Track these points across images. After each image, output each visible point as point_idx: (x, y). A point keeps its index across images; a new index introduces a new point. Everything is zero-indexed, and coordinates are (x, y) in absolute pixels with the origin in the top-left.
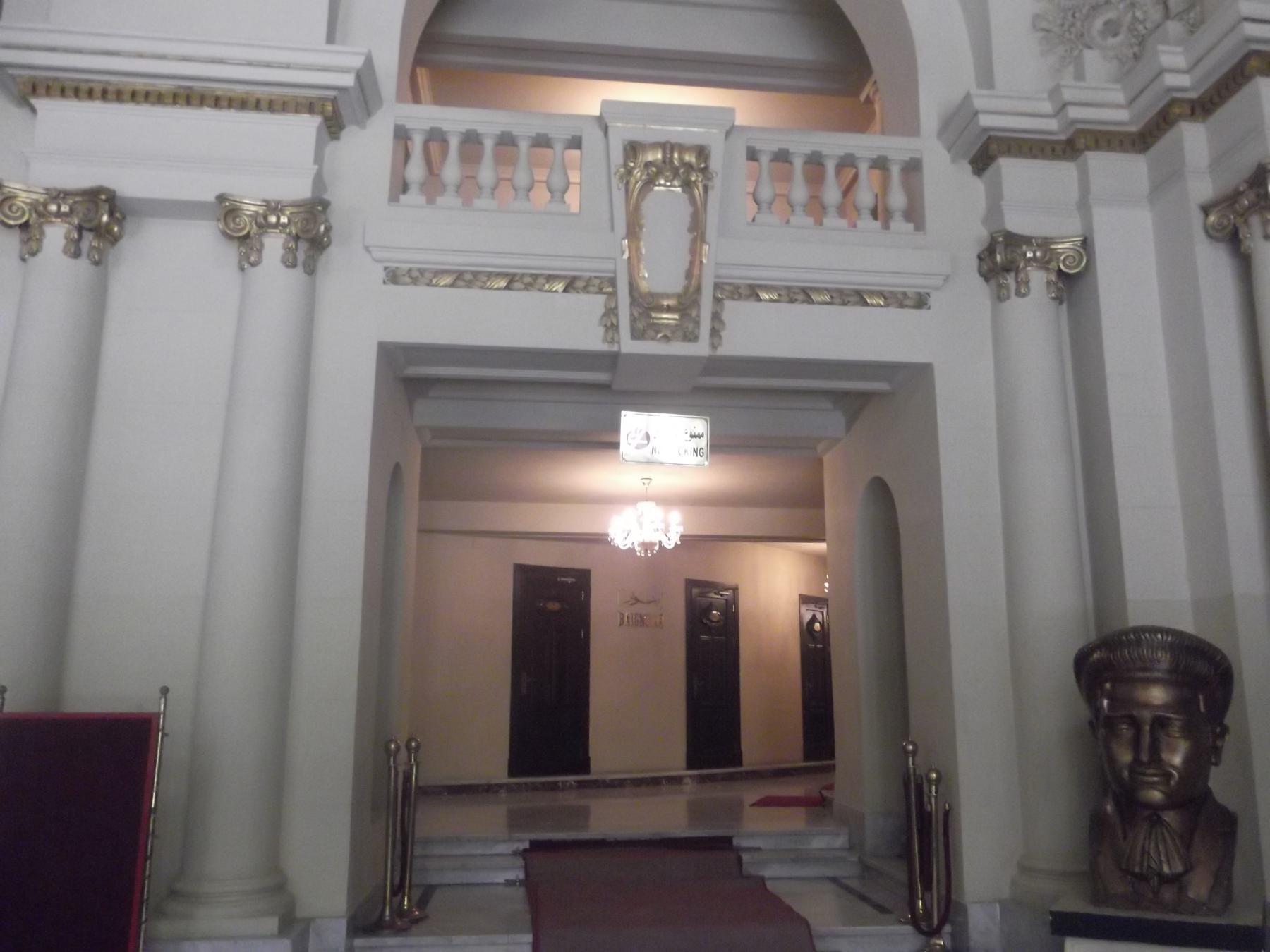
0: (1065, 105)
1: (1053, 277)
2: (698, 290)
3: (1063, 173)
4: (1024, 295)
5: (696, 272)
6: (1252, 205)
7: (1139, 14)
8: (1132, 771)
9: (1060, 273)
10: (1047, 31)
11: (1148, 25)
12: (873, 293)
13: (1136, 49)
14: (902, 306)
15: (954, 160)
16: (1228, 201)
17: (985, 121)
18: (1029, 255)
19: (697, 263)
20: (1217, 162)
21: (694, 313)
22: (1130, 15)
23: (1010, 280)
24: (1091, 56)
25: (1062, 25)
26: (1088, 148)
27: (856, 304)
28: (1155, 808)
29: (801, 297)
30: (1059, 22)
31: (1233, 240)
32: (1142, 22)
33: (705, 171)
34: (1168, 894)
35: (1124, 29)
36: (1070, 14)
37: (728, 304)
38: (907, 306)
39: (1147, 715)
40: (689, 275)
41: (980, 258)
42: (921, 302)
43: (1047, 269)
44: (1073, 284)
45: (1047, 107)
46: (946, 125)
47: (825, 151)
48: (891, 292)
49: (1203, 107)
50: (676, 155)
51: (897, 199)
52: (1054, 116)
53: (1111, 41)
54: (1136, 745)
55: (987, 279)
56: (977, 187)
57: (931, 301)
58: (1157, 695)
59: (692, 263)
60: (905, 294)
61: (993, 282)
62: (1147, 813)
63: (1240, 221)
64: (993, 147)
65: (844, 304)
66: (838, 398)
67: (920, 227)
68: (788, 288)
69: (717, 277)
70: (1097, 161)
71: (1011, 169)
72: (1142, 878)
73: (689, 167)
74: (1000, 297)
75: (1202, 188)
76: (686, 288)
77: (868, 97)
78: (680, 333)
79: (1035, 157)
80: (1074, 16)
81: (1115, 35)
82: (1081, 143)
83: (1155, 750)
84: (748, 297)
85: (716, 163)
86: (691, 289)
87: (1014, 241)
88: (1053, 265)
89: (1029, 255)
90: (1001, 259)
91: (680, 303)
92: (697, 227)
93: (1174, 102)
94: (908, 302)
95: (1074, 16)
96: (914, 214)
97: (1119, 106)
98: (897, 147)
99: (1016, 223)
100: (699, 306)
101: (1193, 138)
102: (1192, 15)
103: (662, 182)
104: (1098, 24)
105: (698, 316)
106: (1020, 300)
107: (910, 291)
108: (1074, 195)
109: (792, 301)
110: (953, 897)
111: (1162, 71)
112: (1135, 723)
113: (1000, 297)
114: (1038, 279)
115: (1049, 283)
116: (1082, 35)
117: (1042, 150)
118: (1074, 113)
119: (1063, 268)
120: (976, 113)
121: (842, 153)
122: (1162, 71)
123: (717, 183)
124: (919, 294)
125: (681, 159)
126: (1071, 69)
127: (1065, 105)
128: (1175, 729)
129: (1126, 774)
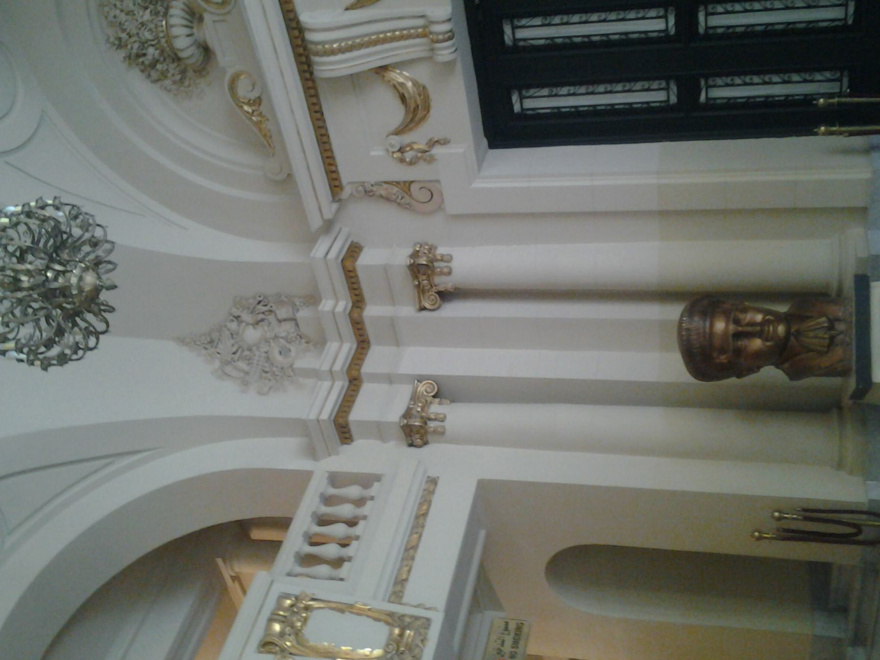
0: (331, 371)
1: (437, 400)
2: (391, 615)
3: (367, 388)
4: (445, 417)
5: (376, 615)
6: (428, 280)
7: (283, 335)
8: (767, 340)
9: (434, 397)
10: (270, 388)
11: (292, 330)
12: (419, 508)
13: (303, 341)
14: (433, 492)
15: (337, 454)
16: (421, 290)
17: (325, 416)
18: (419, 409)
19: (370, 613)
20: (393, 301)
21: (408, 620)
22: (281, 341)
23: (432, 425)
24: (298, 364)
25: (270, 380)
26: (359, 370)
27: (425, 519)
28: (788, 333)
29: (411, 552)
30: (267, 381)
31: (445, 296)
32: (288, 333)
33: (297, 598)
34: (841, 327)
35: (288, 346)
36: (264, 375)
37: (405, 600)
38: (434, 490)
39: (732, 328)
40: (377, 620)
41: (411, 445)
42: (433, 481)
43: (431, 403)
44: (443, 391)
45: (327, 384)
46: (312, 453)
47: (305, 528)
48: (422, 497)
49: (358, 301)
50: (281, 613)
51: (354, 491)
52: (333, 381)
53: (293, 354)
54: (750, 335)
55: (426, 443)
56: (360, 444)
57: (432, 473)
58: (720, 326)
59: (368, 616)
60: (425, 490)
61: (430, 438)
62: (792, 339)
63: (434, 289)
64: (341, 421)
65: (423, 527)
66: (476, 605)
67: (378, 478)
68: (403, 559)
69: (383, 600)
70: (369, 366)
71: (358, 414)
72: (832, 339)
73: (292, 606)
74: (440, 433)
75: (407, 311)
76: (387, 623)
77: (231, 577)
78: (422, 631)
79: (353, 402)
80: (266, 372)
81: (290, 350)
82: (354, 373)
83: (752, 324)
84: (403, 586)
85: (296, 591)
86: (390, 620)
87: (408, 414)
88: (429, 399)
89: (419, 409)
90: (415, 432)
91: (399, 626)
92: (343, 608)
93: (350, 314)
94: (431, 489)
95: (266, 372)
96: (367, 481)
97: (340, 348)
98: (317, 486)
99: (395, 414)
100: (403, 616)
101: (372, 311)
102: (298, 304)
103: (299, 624)
104: (279, 358)
105: (411, 617)
106: (447, 421)
107: (424, 486)
108: (384, 387)
109: (413, 558)
110: (865, 509)
111: (333, 312)
112: (737, 335)
113: (440, 433)
114: (435, 408)
115: (440, 404)
116: (282, 368)
117: (352, 396)
118: (338, 367)
119: (433, 394)
120: (318, 421)
121: (309, 519)
122: (333, 312)
123: (310, 592)
124: (427, 482)
125: (285, 610)
126: (301, 379)
127: (331, 371)
128: (741, 316)
129: (768, 344)
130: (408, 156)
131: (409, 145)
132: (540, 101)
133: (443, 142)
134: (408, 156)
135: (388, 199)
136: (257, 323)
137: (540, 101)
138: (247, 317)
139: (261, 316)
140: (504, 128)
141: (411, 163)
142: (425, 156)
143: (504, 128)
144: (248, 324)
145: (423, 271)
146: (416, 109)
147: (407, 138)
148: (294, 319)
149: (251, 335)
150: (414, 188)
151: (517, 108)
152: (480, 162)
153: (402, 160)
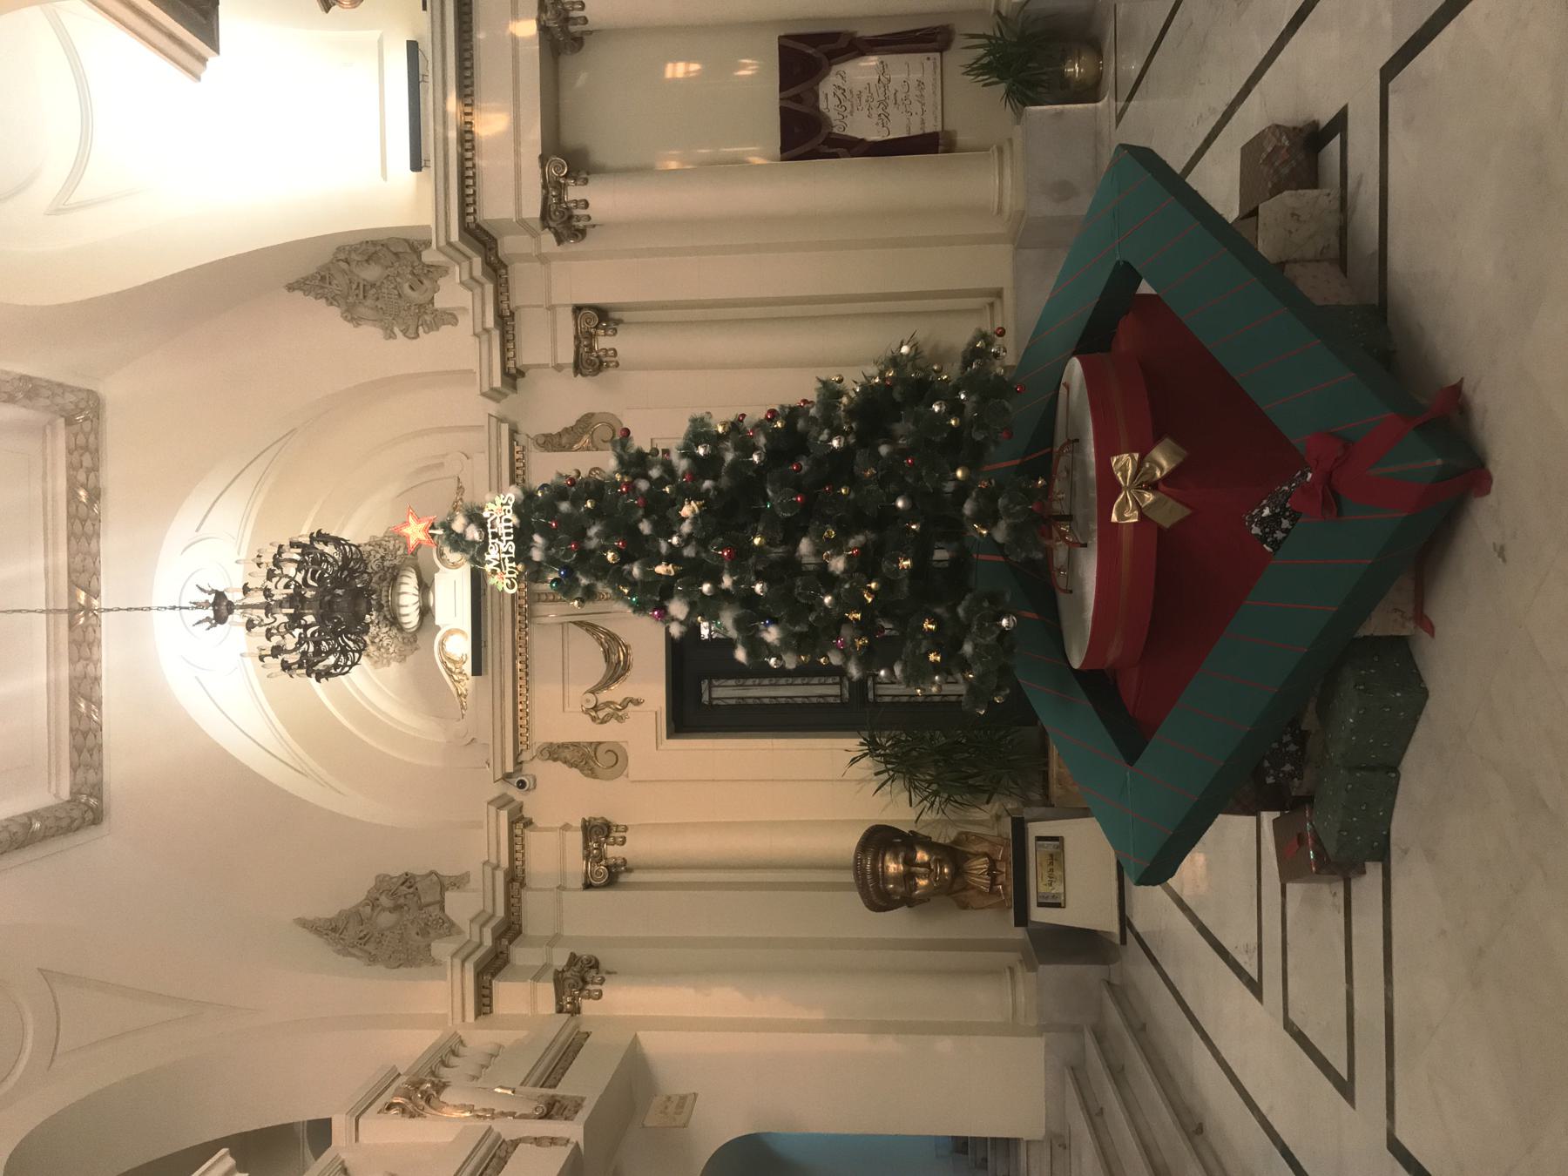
130: (601, 714)
131: (608, 704)
132: (725, 692)
133: (637, 702)
134: (601, 714)
135: (572, 765)
136: (397, 908)
137: (725, 692)
138: (385, 901)
139: (402, 901)
140: (687, 715)
141: (603, 722)
142: (617, 712)
143: (687, 715)
144: (384, 909)
145: (597, 831)
146: (617, 670)
147: (604, 696)
148: (441, 904)
149: (386, 919)
150: (601, 749)
151: (705, 698)
152: (668, 737)
153: (594, 719)
